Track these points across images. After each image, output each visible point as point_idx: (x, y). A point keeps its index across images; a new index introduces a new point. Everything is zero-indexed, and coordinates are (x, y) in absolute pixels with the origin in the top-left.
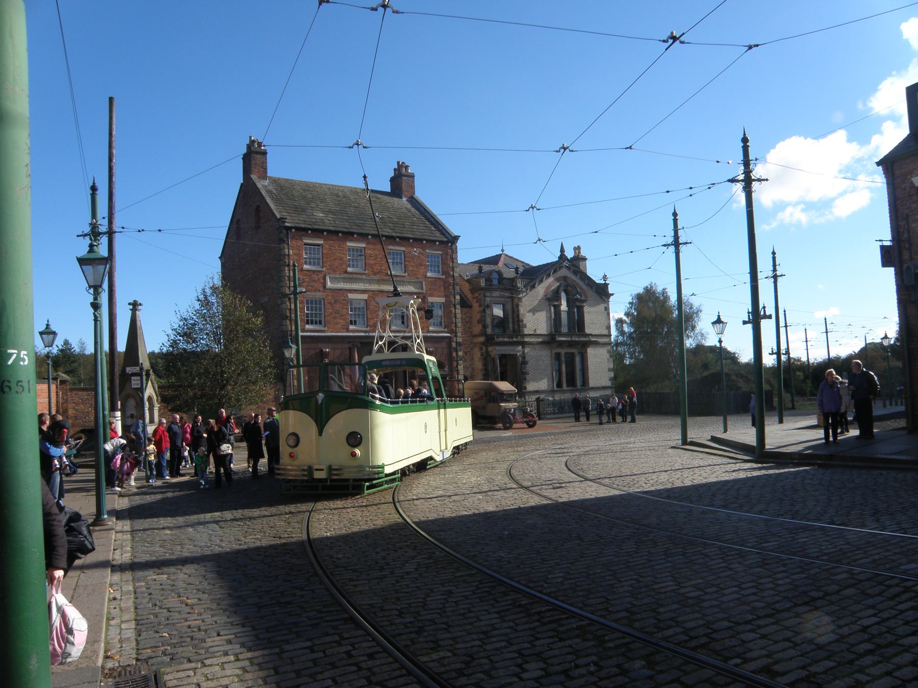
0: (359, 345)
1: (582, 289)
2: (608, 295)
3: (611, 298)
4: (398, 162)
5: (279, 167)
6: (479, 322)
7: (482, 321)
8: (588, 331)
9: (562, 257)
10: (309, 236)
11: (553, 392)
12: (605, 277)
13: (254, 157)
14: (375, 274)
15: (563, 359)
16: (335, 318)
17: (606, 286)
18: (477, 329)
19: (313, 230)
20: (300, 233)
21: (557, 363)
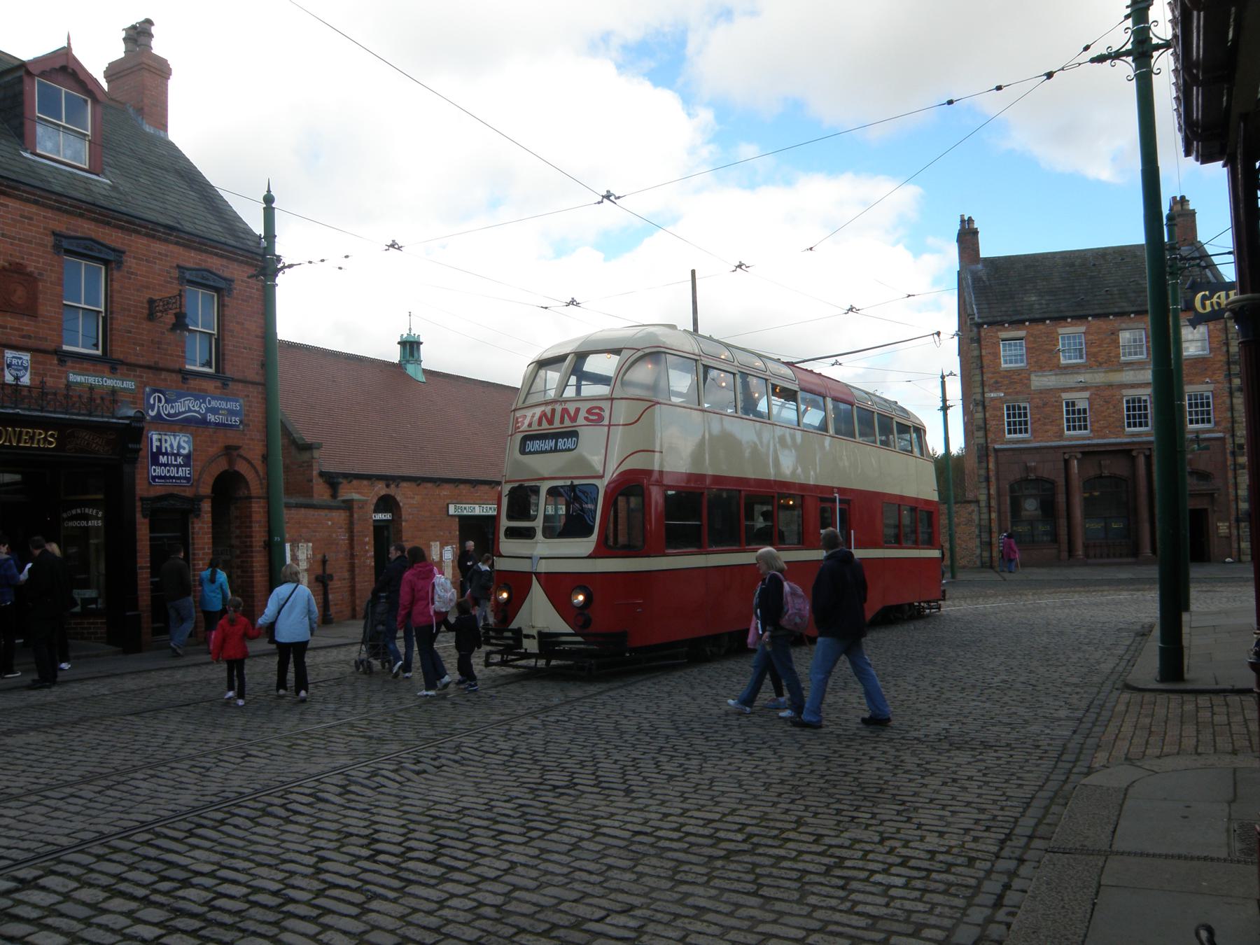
0: (1079, 456)
10: (1006, 330)
14: (1101, 364)
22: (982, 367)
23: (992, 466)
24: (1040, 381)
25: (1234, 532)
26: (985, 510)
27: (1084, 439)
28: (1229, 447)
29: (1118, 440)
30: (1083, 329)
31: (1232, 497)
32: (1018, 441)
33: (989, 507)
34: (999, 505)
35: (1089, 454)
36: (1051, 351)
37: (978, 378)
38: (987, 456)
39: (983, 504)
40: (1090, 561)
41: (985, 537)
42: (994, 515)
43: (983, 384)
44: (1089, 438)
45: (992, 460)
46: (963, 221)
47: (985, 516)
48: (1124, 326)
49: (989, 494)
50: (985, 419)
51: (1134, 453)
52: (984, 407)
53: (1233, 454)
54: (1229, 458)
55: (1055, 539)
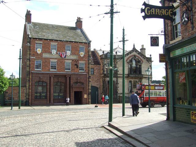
0: (54, 76)
1: (141, 59)
2: (151, 61)
3: (153, 63)
4: (78, 17)
5: (34, 19)
6: (102, 69)
7: (103, 69)
8: (143, 73)
9: (134, 48)
10: (37, 41)
11: (128, 94)
12: (151, 55)
13: (28, 16)
15: (132, 83)
16: (45, 67)
17: (150, 58)
18: (102, 72)
19: (39, 39)
20: (34, 40)
21: (130, 84)
22: (30, 50)
23: (30, 77)
24: (45, 55)
25: (88, 97)
26: (28, 89)
27: (55, 72)
28: (88, 76)
29: (63, 73)
30: (57, 43)
31: (88, 89)
32: (38, 71)
33: (29, 88)
34: (32, 88)
35: (56, 76)
36: (48, 48)
37: (29, 52)
38: (30, 74)
39: (27, 87)
40: (55, 104)
41: (27, 96)
42: (30, 91)
43: (30, 54)
44: (56, 72)
45: (31, 75)
46: (27, 11)
47: (28, 91)
48: (66, 44)
49: (29, 85)
50: (30, 64)
51: (67, 76)
52: (30, 61)
53: (88, 78)
54: (88, 79)
55: (46, 97)
